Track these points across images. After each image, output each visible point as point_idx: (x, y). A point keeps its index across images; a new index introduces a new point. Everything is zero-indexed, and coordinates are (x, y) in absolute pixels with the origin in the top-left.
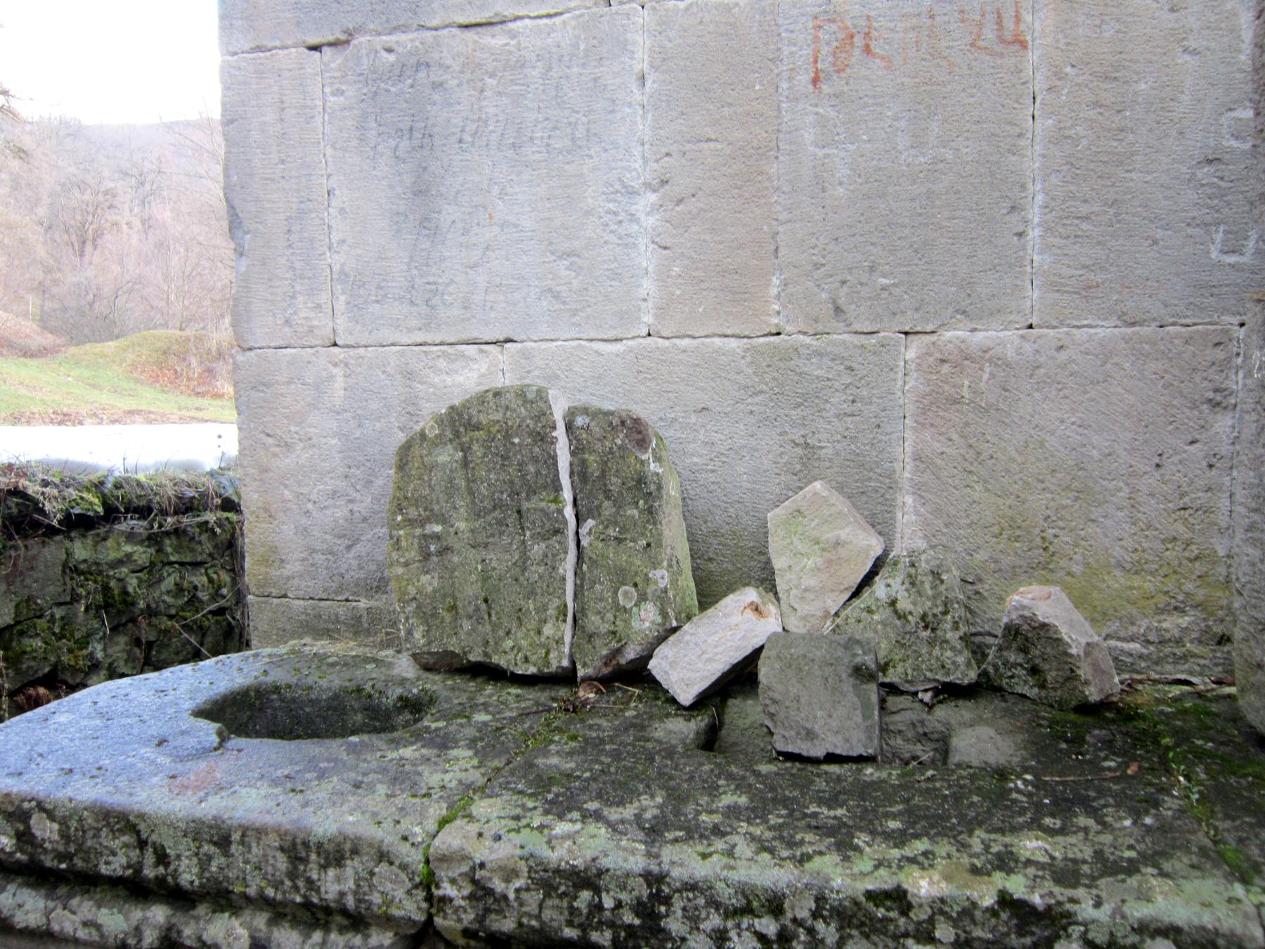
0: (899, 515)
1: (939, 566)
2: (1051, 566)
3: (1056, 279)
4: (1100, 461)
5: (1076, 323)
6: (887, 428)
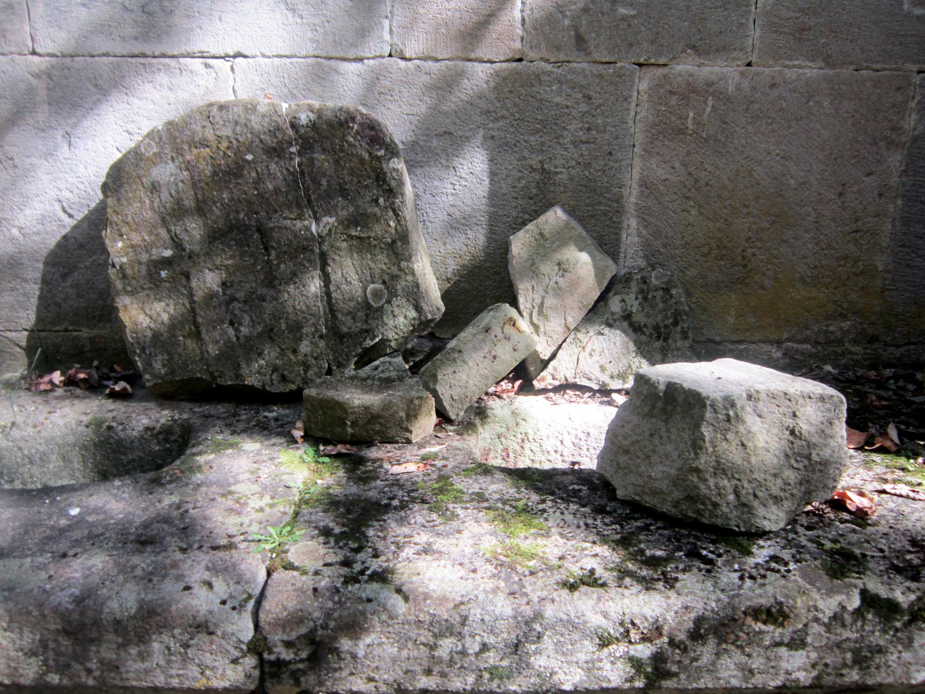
0: (624, 236)
1: (667, 283)
2: (747, 281)
3: (776, 20)
4: (796, 189)
6: (619, 156)
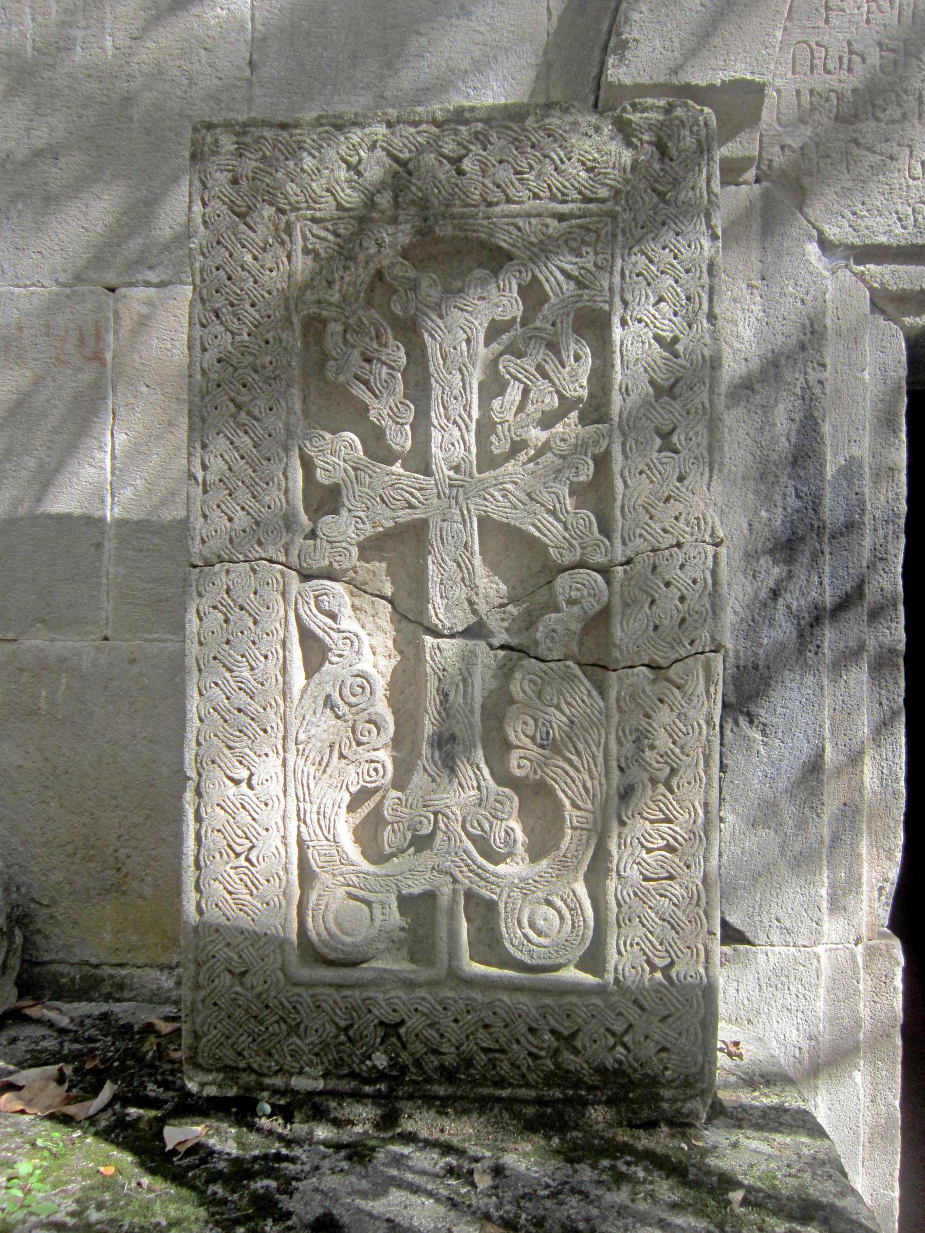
2: (124, 888)
5: (146, 636)
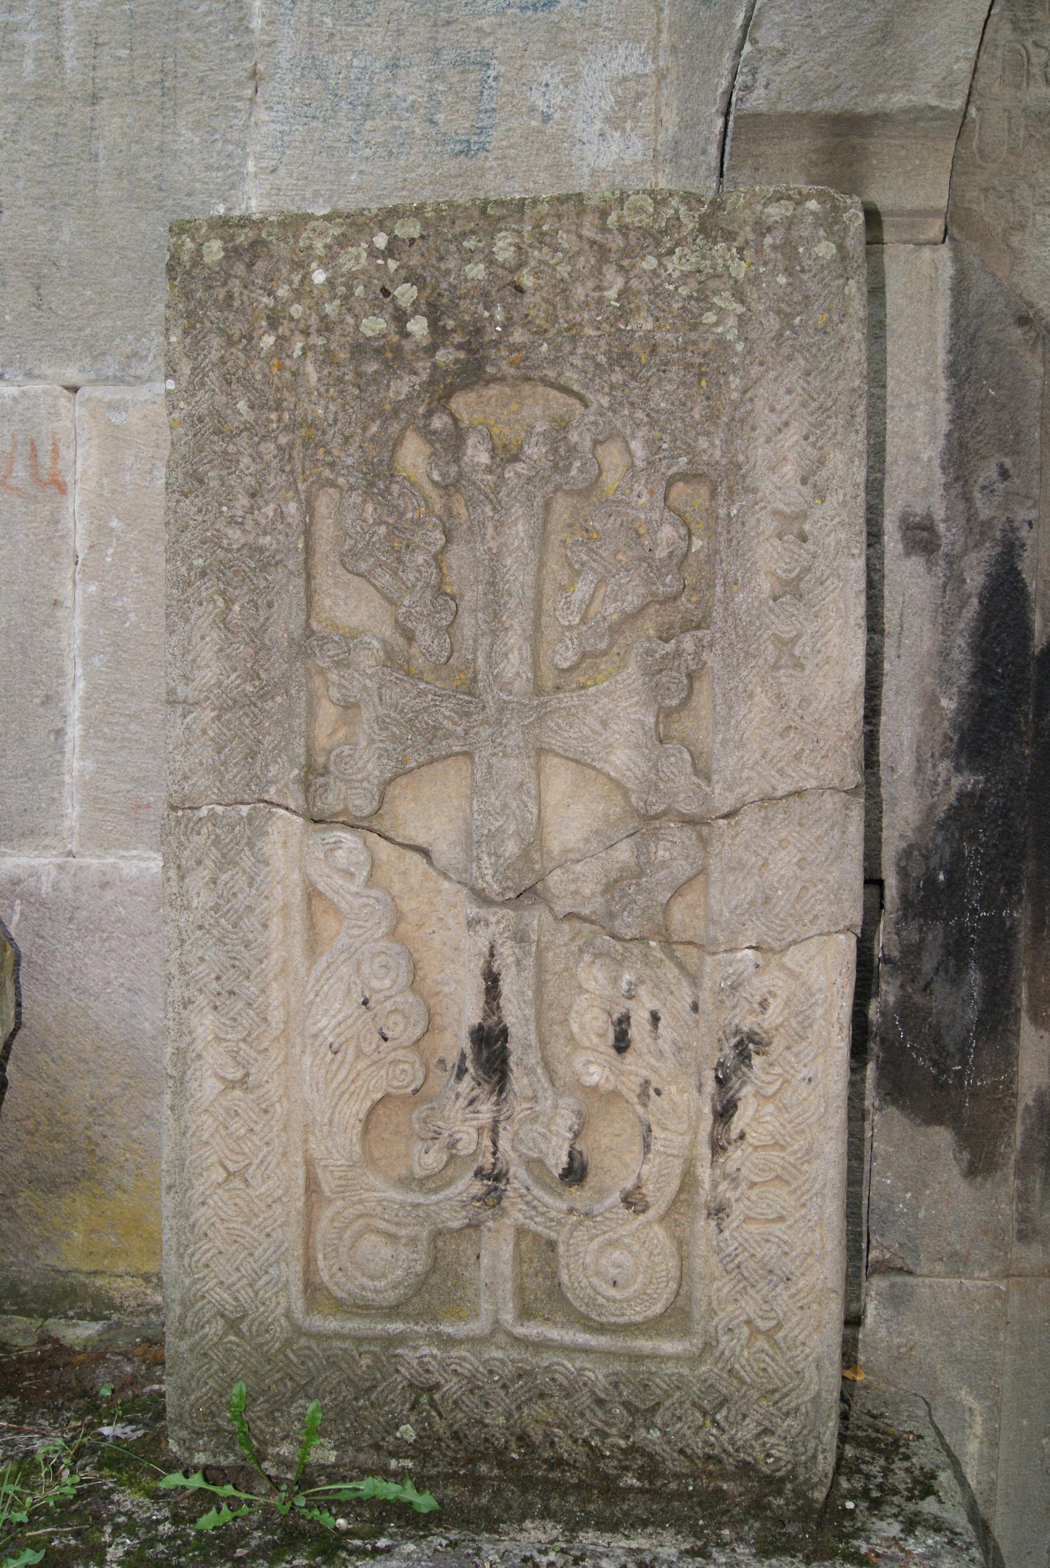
4: (154, 1038)
5: (124, 853)
